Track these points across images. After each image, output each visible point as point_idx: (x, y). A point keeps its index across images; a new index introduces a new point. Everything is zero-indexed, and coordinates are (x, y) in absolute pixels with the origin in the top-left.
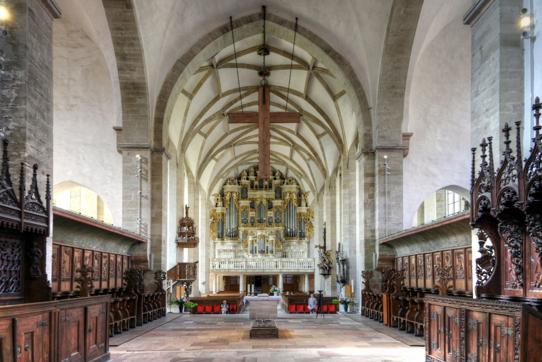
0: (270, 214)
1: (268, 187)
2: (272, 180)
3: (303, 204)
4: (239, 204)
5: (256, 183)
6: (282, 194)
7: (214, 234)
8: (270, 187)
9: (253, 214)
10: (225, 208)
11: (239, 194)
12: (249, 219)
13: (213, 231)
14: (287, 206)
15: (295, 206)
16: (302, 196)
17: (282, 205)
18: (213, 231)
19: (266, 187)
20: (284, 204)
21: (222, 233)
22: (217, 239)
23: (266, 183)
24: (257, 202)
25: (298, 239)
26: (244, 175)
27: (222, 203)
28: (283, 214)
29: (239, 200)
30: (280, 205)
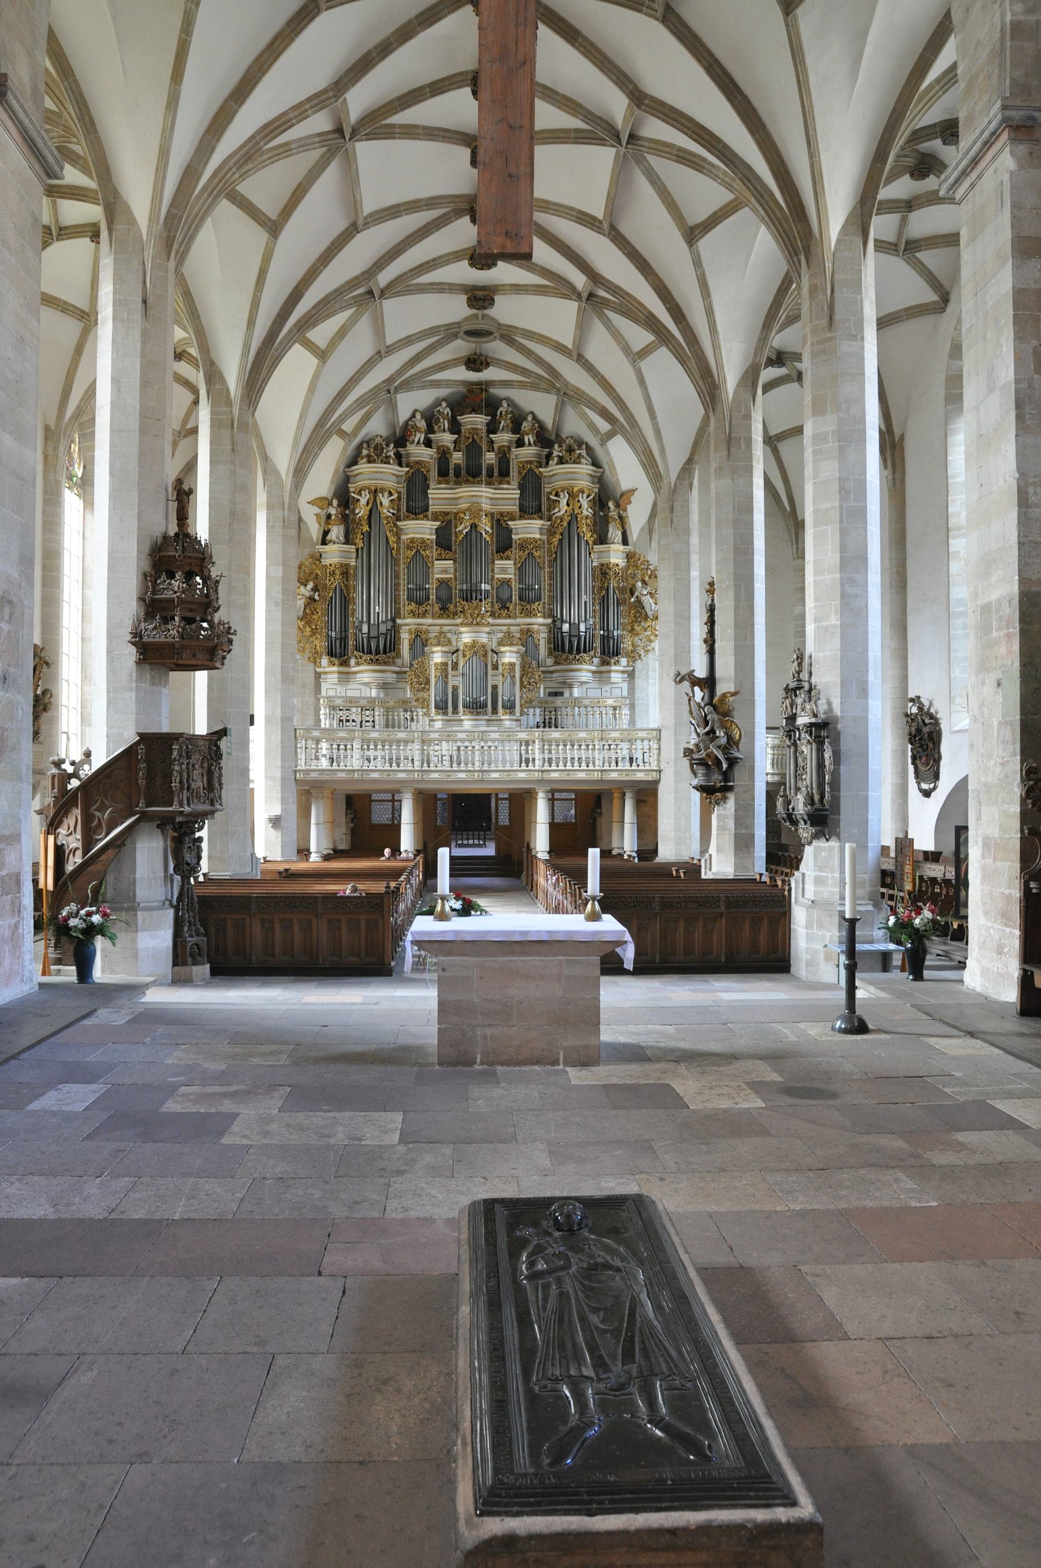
0: (504, 570)
2: (509, 448)
3: (614, 533)
4: (398, 533)
5: (457, 457)
6: (544, 499)
7: (317, 643)
8: (504, 473)
9: (445, 572)
10: (353, 548)
11: (399, 498)
12: (432, 586)
13: (314, 632)
14: (561, 540)
16: (611, 505)
17: (545, 537)
18: (314, 632)
19: (490, 474)
20: (551, 532)
21: (344, 640)
22: (325, 661)
24: (460, 528)
26: (417, 429)
27: (342, 527)
29: (399, 520)
30: (538, 536)
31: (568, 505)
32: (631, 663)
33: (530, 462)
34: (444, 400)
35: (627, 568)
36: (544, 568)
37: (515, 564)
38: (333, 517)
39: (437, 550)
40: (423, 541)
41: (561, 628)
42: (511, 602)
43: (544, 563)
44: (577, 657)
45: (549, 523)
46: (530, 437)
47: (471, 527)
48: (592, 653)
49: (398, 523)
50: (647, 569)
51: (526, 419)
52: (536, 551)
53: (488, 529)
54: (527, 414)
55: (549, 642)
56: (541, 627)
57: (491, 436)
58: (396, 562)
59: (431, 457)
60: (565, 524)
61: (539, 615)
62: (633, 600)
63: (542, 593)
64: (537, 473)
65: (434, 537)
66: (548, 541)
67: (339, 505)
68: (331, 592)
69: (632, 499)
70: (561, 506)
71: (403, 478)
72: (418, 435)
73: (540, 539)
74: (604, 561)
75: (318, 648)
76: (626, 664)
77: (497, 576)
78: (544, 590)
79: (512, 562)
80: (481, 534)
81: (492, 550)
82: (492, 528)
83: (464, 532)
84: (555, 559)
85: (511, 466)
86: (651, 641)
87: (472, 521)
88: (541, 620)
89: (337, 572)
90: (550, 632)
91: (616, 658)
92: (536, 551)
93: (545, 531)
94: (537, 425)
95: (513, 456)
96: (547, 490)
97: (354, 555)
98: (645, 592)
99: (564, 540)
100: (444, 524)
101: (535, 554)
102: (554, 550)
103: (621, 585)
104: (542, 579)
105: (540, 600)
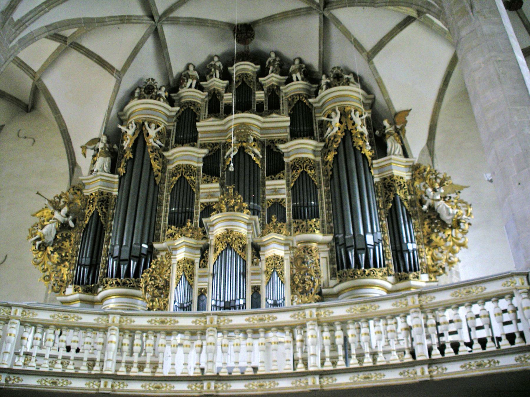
0: (276, 191)
1: (266, 108)
2: (278, 88)
3: (393, 145)
4: (165, 162)
5: (229, 98)
6: (316, 127)
7: (65, 271)
10: (116, 178)
13: (62, 260)
14: (336, 157)
15: (364, 156)
16: (386, 123)
17: (319, 159)
18: (62, 260)
22: (70, 290)
23: (260, 96)
25: (391, 279)
27: (108, 160)
28: (323, 188)
29: (166, 150)
30: (311, 156)
31: (341, 122)
32: (433, 279)
33: (299, 95)
34: (216, 56)
35: (413, 179)
36: (320, 188)
37: (288, 185)
38: (100, 150)
39: (203, 176)
40: (188, 168)
41: (344, 244)
42: (285, 221)
43: (320, 182)
44: (367, 271)
45: (322, 144)
46: (298, 75)
47: (239, 150)
49: (165, 154)
50: (436, 179)
51: (294, 64)
53: (257, 151)
54: (294, 60)
55: (331, 262)
56: (321, 247)
57: (260, 79)
58: (157, 189)
59: (203, 100)
60: (340, 140)
62: (425, 207)
64: (307, 104)
65: (201, 165)
66: (323, 161)
67: (108, 142)
68: (88, 219)
69: (408, 118)
70: (333, 124)
71: (175, 119)
72: (190, 81)
74: (386, 174)
75: (65, 277)
76: (428, 280)
77: (268, 197)
78: (322, 208)
79: (284, 182)
80: (250, 156)
81: (263, 174)
82: (262, 154)
83: (232, 156)
84: (332, 176)
85: (281, 102)
86: (454, 252)
87: (240, 144)
88: (318, 236)
89: (96, 200)
90: (331, 251)
91: (415, 273)
92: (311, 170)
93: (319, 154)
94: (304, 66)
95: (282, 94)
96: (318, 119)
97: (116, 186)
98: (438, 197)
100: (212, 153)
101: (309, 172)
102: (329, 168)
103: (409, 197)
104: (319, 198)
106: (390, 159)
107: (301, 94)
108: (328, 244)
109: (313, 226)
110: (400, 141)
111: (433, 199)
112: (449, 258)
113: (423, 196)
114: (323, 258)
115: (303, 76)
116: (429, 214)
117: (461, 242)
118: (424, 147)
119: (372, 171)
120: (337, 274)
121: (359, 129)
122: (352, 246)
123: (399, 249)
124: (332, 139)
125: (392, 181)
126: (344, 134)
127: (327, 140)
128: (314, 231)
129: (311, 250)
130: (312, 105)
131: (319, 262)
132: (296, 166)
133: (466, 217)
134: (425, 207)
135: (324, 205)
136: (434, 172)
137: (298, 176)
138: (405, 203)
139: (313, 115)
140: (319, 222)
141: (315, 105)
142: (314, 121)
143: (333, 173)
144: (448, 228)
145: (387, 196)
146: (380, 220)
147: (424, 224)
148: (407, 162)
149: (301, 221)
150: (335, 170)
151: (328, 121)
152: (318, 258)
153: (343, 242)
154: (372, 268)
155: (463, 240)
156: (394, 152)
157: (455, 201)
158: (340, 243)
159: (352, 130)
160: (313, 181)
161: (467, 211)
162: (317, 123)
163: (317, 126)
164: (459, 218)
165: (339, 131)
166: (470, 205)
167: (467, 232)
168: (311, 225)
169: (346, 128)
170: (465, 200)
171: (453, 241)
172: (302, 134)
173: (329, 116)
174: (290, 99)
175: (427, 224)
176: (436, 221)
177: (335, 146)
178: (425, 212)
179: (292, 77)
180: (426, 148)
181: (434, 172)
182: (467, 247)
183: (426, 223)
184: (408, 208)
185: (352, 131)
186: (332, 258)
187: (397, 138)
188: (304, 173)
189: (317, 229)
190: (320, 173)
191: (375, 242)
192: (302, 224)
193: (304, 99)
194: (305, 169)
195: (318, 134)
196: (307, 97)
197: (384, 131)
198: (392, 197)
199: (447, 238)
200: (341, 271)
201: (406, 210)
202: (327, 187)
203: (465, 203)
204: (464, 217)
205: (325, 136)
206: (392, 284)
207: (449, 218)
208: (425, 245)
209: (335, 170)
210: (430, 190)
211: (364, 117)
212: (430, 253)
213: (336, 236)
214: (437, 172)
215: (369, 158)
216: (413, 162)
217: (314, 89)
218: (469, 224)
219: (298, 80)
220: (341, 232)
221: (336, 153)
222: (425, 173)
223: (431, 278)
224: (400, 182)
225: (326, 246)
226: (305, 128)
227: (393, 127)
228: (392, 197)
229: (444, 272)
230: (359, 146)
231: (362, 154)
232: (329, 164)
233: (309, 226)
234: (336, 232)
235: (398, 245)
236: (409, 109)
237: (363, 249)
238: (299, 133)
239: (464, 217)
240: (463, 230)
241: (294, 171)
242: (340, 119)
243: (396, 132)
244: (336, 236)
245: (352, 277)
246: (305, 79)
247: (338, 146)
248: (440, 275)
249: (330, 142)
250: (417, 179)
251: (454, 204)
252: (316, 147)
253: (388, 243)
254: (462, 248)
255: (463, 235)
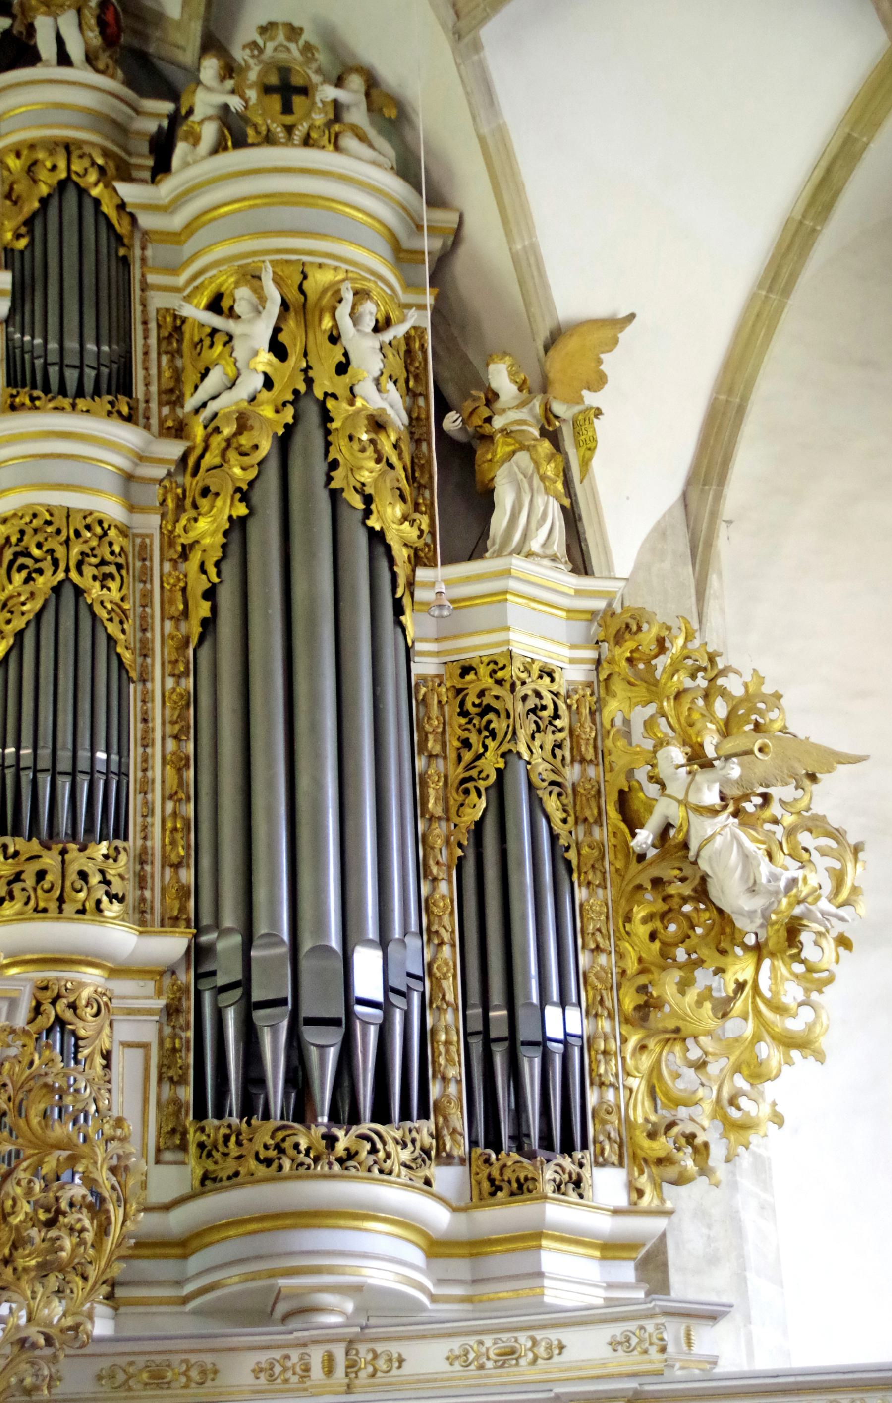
14: (238, 526)
15: (377, 538)
33: (68, 147)
41: (245, 983)
43: (145, 652)
45: (174, 449)
46: (68, 24)
48: (424, 1130)
50: (706, 696)
52: (104, 580)
56: (123, 987)
60: (266, 446)
61: (112, 910)
62: (644, 838)
63: (135, 802)
64: (108, 208)
66: (169, 540)
69: (610, 362)
70: (240, 350)
73: (124, 531)
76: (622, 1200)
78: (145, 788)
84: (209, 625)
90: (172, 1011)
91: (566, 1162)
92: (104, 580)
96: (158, 301)
98: (711, 797)
99: (254, 529)
101: (95, 591)
104: (135, 729)
105: (121, 833)
106: (507, 573)
107: (80, 144)
108: (161, 974)
109: (95, 879)
110: (560, 486)
111: (684, 803)
112: (733, 1102)
113: (641, 774)
114: (127, 1045)
115: (94, 37)
116: (655, 872)
117: (794, 1025)
118: (670, 511)
119: (406, 619)
120: (193, 1137)
121: (367, 391)
122: (283, 1002)
123: (499, 1030)
124: (227, 431)
125: (500, 683)
126: (288, 415)
127: (199, 433)
128: (98, 908)
129: (73, 1006)
130: (133, 218)
131: (107, 1066)
132: (29, 555)
133: (832, 908)
134: (644, 838)
135: (157, 772)
136: (705, 663)
137: (31, 607)
138: (552, 804)
139: (136, 272)
140: (123, 858)
141: (145, 221)
142: (137, 309)
143: (214, 609)
144: (738, 951)
145: (468, 756)
146: (422, 871)
147: (628, 919)
148: (579, 593)
149: (34, 846)
150: (227, 597)
151: (214, 331)
152: (106, 1045)
153: (238, 976)
154: (366, 1126)
155: (806, 1014)
156: (525, 536)
157: (789, 820)
158: (221, 980)
159: (334, 396)
160: (111, 641)
161: (839, 879)
162: (153, 326)
163: (153, 341)
164: (798, 910)
165: (265, 395)
166: (857, 849)
167: (830, 980)
168: (83, 875)
169: (302, 388)
170: (834, 820)
171: (758, 1013)
172: (72, 376)
173: (215, 305)
174: (12, 162)
175: (645, 921)
176: (687, 908)
177: (237, 471)
178: (641, 858)
179: (31, 29)
180: (680, 513)
181: (705, 663)
182: (820, 1057)
183: (639, 913)
184: (558, 827)
185: (330, 404)
186: (174, 1050)
187: (550, 470)
188: (68, 594)
189: (112, 897)
190: (146, 599)
191: (388, 989)
192: (36, 866)
193: (92, 177)
194: (74, 575)
195: (154, 389)
196: (111, 169)
197: (488, 420)
198: (491, 763)
199: (730, 1000)
200: (211, 1122)
201: (554, 838)
202: (178, 677)
203: (837, 835)
204: (824, 904)
205: (191, 403)
206: (455, 1210)
207: (757, 903)
208: (627, 1020)
209: (227, 597)
210: (677, 754)
211: (398, 331)
212: (646, 1061)
213: (204, 939)
214: (721, 663)
215: (401, 554)
216: (609, 596)
217: (151, 126)
218: (843, 942)
219: (64, 59)
220: (229, 920)
221: (241, 510)
222: (662, 662)
223: (640, 1193)
224: (538, 695)
225: (150, 987)
226: (91, 347)
227: (537, 405)
228: (491, 763)
229: (704, 1171)
230: (360, 490)
231: (371, 530)
232: (196, 558)
233: (72, 876)
234: (206, 921)
235: (498, 1014)
236: (622, 314)
237: (334, 1022)
238: (53, 371)
239: (824, 904)
240: (811, 969)
241: (18, 578)
242: (277, 330)
243: (544, 433)
244: (204, 939)
245: (268, 1162)
246: (103, 60)
247: (252, 474)
248: (681, 1180)
249: (217, 442)
250: (618, 686)
251: (779, 832)
252: (141, 458)
253: (450, 997)
254: (795, 1054)
255: (807, 991)
